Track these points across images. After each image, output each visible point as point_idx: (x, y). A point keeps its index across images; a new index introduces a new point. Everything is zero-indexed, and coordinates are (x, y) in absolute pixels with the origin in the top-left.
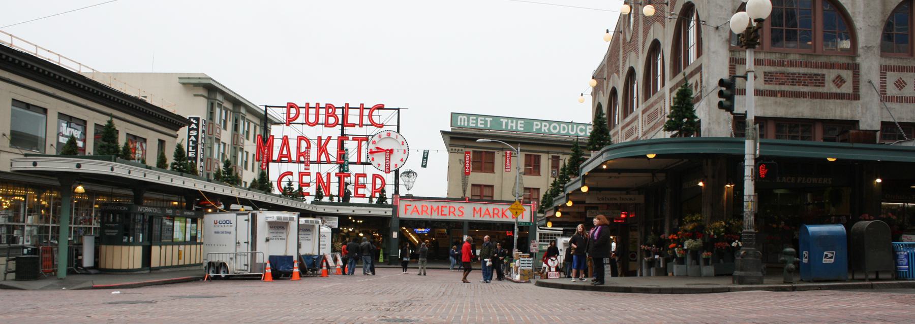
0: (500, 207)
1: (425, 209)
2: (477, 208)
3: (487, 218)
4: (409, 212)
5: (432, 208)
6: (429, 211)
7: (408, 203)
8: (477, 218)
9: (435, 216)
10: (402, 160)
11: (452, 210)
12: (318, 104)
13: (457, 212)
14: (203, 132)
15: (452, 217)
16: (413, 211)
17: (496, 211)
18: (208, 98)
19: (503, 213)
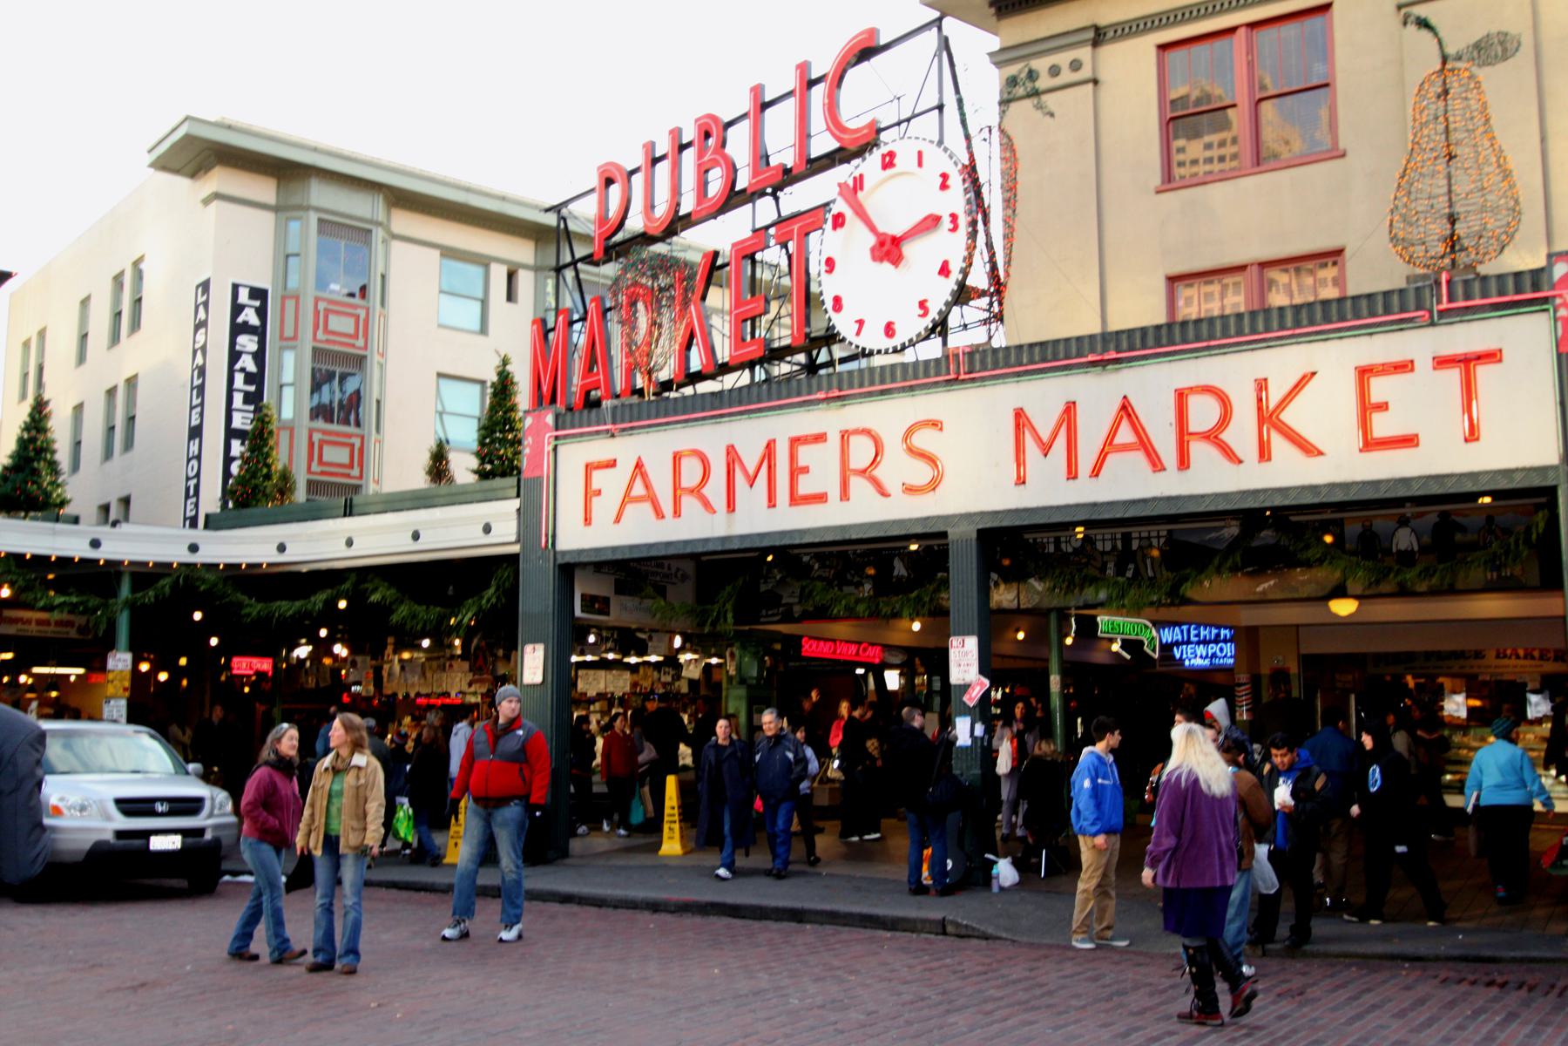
0: (1235, 371)
1: (691, 472)
2: (1045, 420)
3: (1128, 483)
4: (604, 507)
5: (732, 456)
6: (716, 489)
7: (599, 449)
8: (1049, 489)
9: (757, 517)
10: (944, 270)
11: (861, 451)
12: (676, 133)
13: (898, 468)
14: (237, 329)
15: (863, 510)
16: (627, 499)
17: (1203, 414)
18: (276, 209)
19: (1268, 418)
